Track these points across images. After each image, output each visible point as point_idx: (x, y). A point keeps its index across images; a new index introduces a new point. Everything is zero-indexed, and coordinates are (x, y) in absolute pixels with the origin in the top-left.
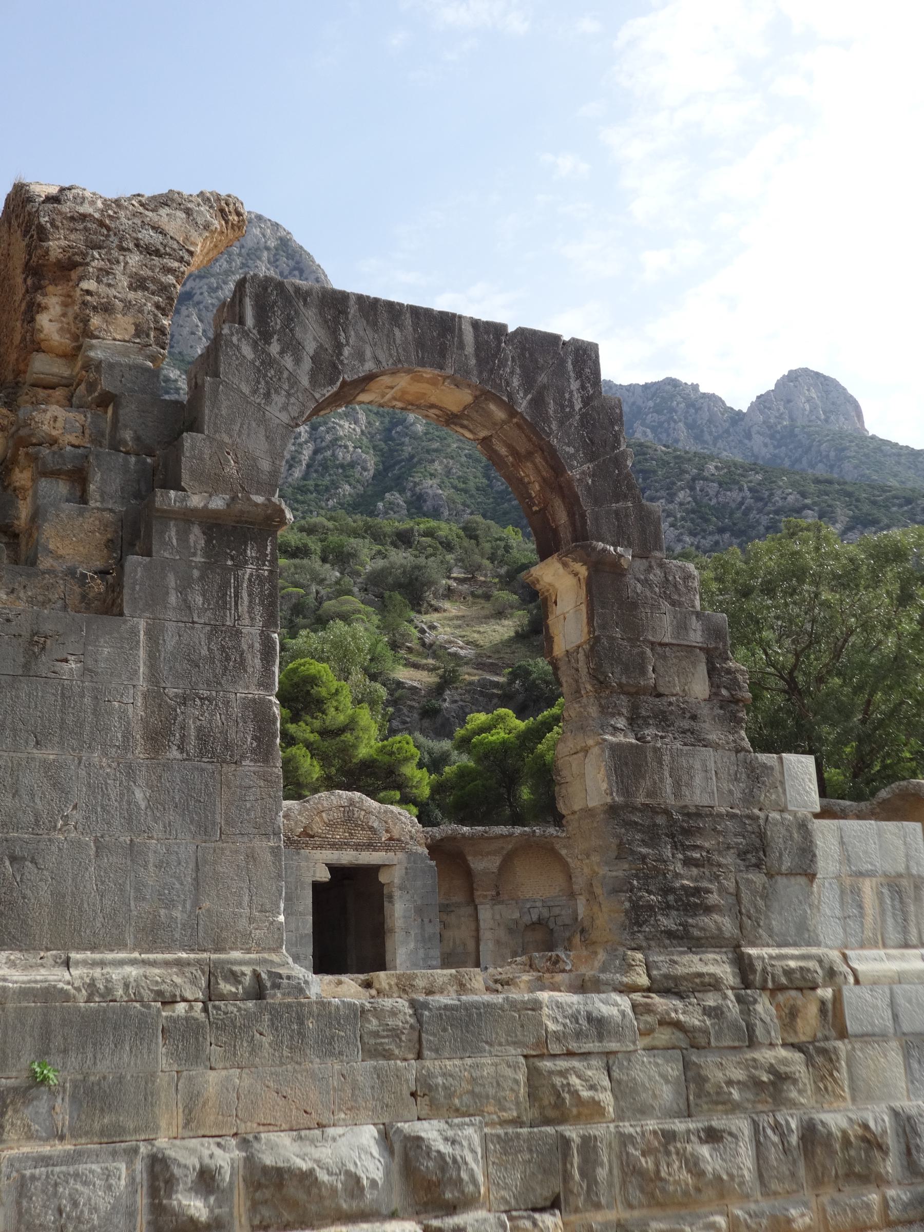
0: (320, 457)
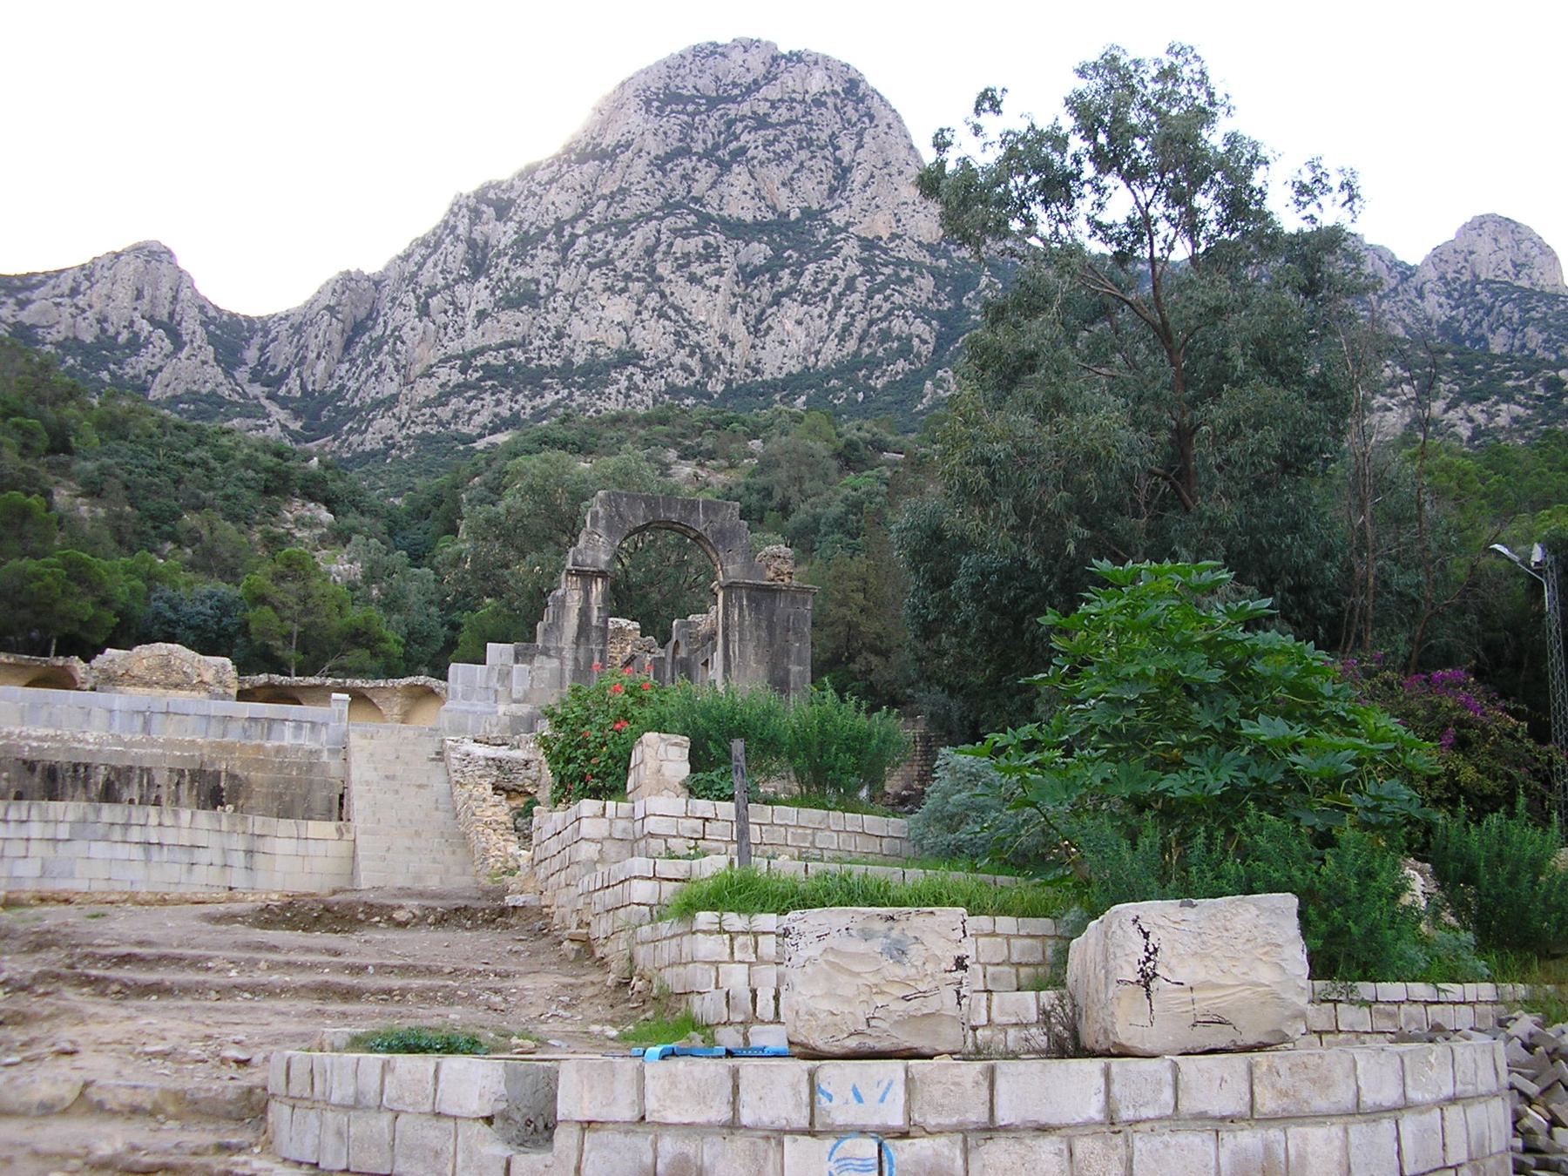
0: (874, 329)
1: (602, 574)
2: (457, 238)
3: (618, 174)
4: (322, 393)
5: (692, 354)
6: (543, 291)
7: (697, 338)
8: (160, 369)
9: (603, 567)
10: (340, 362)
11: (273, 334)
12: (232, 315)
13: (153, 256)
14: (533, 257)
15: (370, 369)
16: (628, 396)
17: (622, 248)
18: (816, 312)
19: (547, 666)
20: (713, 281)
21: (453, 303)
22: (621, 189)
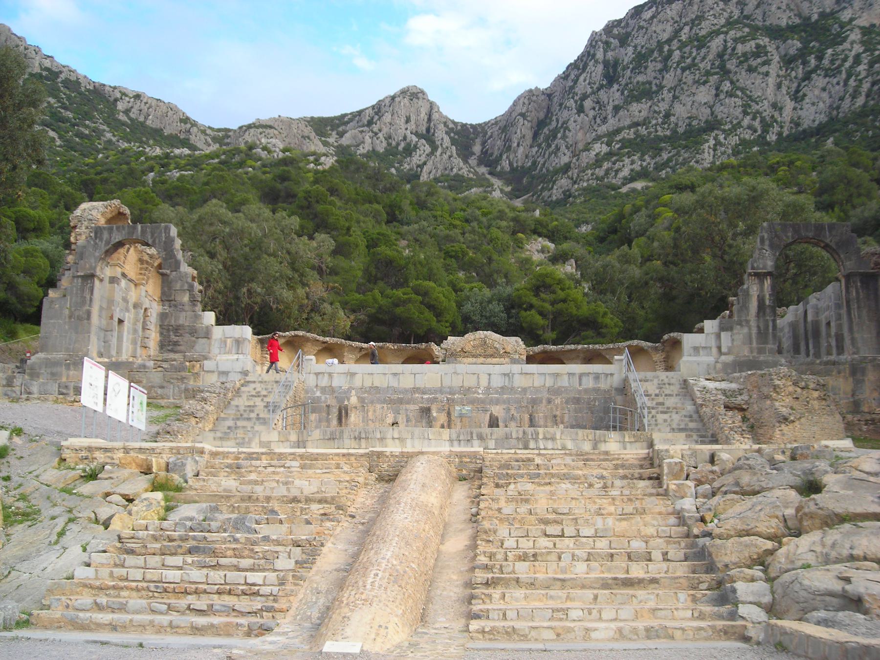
1: (769, 274)
2: (597, 62)
3: (695, 7)
4: (522, 167)
5: (754, 119)
6: (654, 88)
7: (758, 107)
8: (425, 163)
9: (770, 269)
10: (531, 147)
11: (489, 134)
12: (464, 126)
13: (413, 95)
14: (646, 68)
15: (551, 150)
16: (715, 150)
17: (702, 54)
18: (835, 81)
19: (740, 333)
20: (764, 69)
21: (598, 102)
22: (697, 17)
